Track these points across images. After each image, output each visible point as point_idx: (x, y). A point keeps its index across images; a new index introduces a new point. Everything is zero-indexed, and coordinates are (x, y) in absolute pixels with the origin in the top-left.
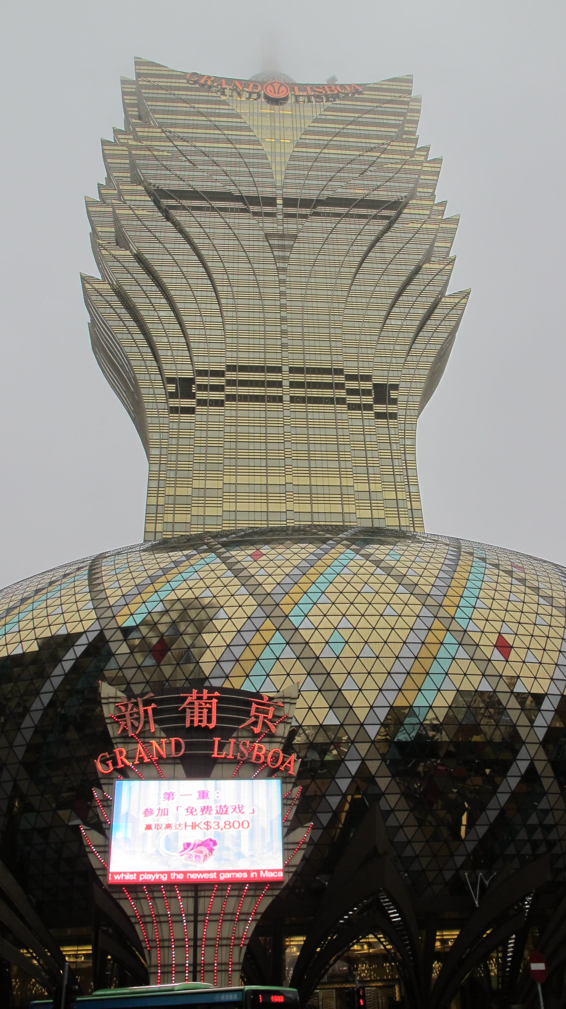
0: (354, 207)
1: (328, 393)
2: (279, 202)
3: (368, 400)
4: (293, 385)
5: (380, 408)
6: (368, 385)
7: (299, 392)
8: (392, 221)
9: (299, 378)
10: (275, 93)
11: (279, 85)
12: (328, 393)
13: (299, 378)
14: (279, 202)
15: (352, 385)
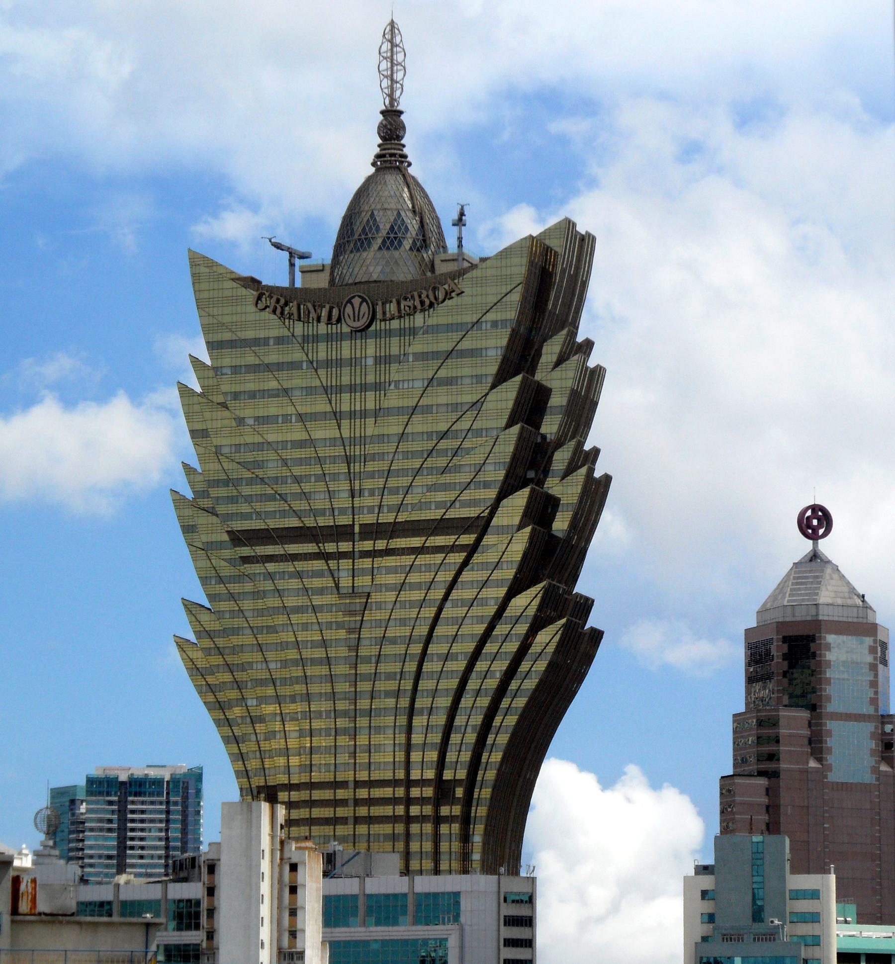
0: (432, 534)
1: (388, 811)
2: (357, 529)
3: (428, 810)
4: (357, 802)
5: (445, 811)
6: (429, 792)
7: (362, 811)
8: (473, 549)
9: (363, 793)
10: (354, 321)
11: (360, 300)
12: (388, 811)
13: (363, 793)
14: (357, 529)
15: (415, 792)
